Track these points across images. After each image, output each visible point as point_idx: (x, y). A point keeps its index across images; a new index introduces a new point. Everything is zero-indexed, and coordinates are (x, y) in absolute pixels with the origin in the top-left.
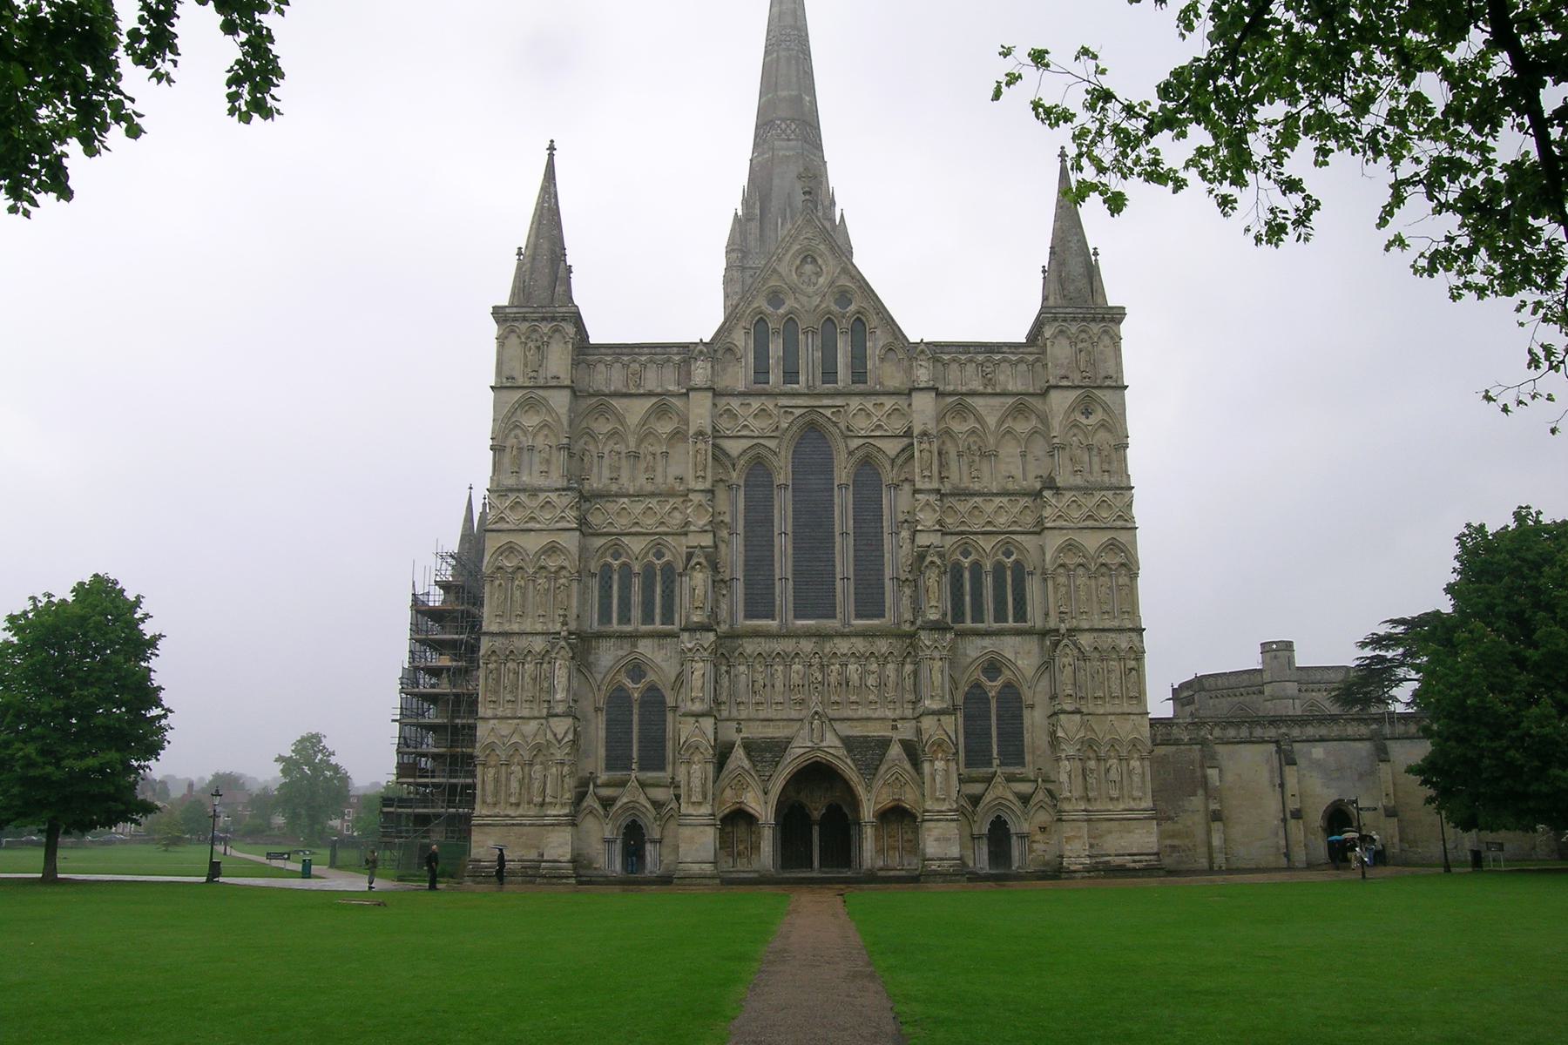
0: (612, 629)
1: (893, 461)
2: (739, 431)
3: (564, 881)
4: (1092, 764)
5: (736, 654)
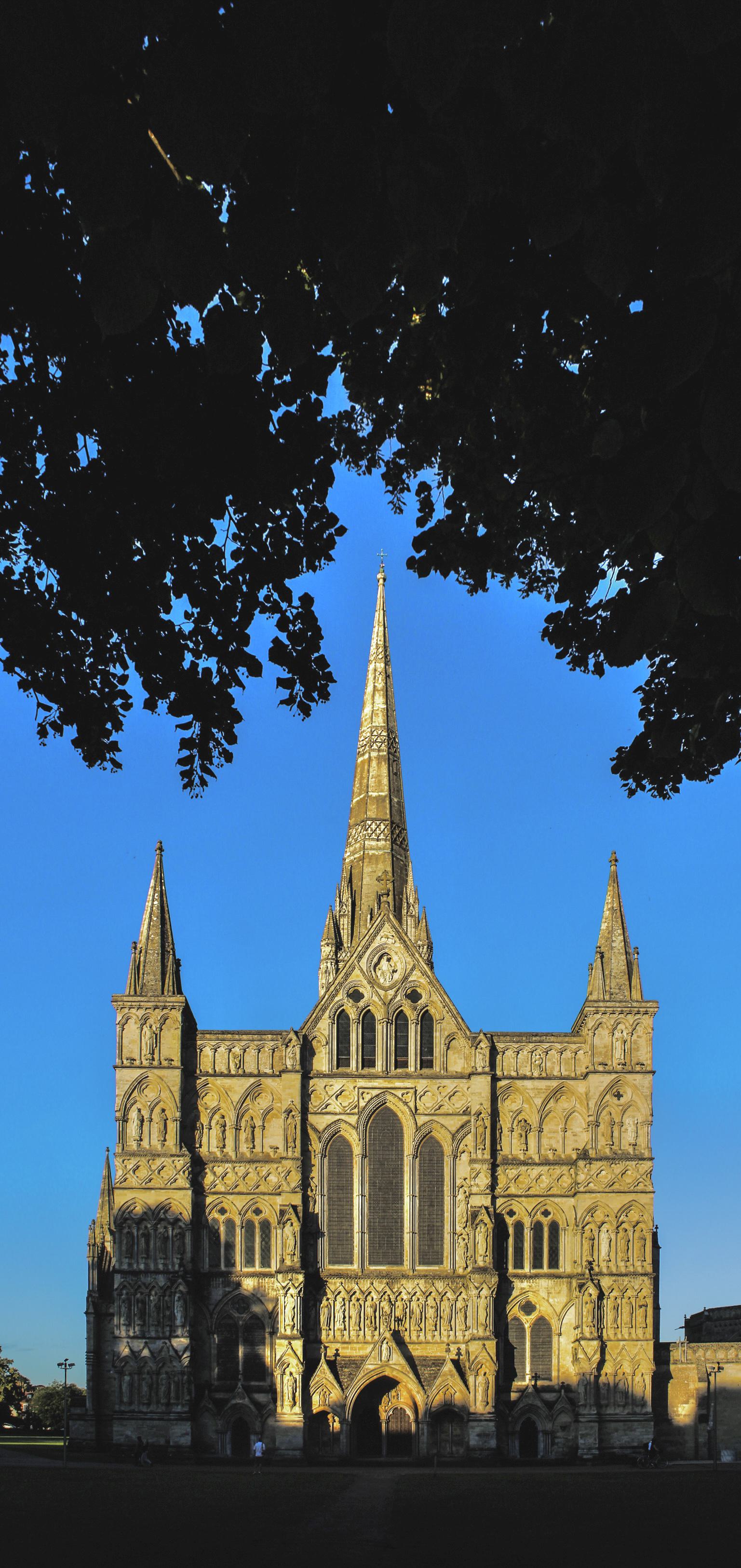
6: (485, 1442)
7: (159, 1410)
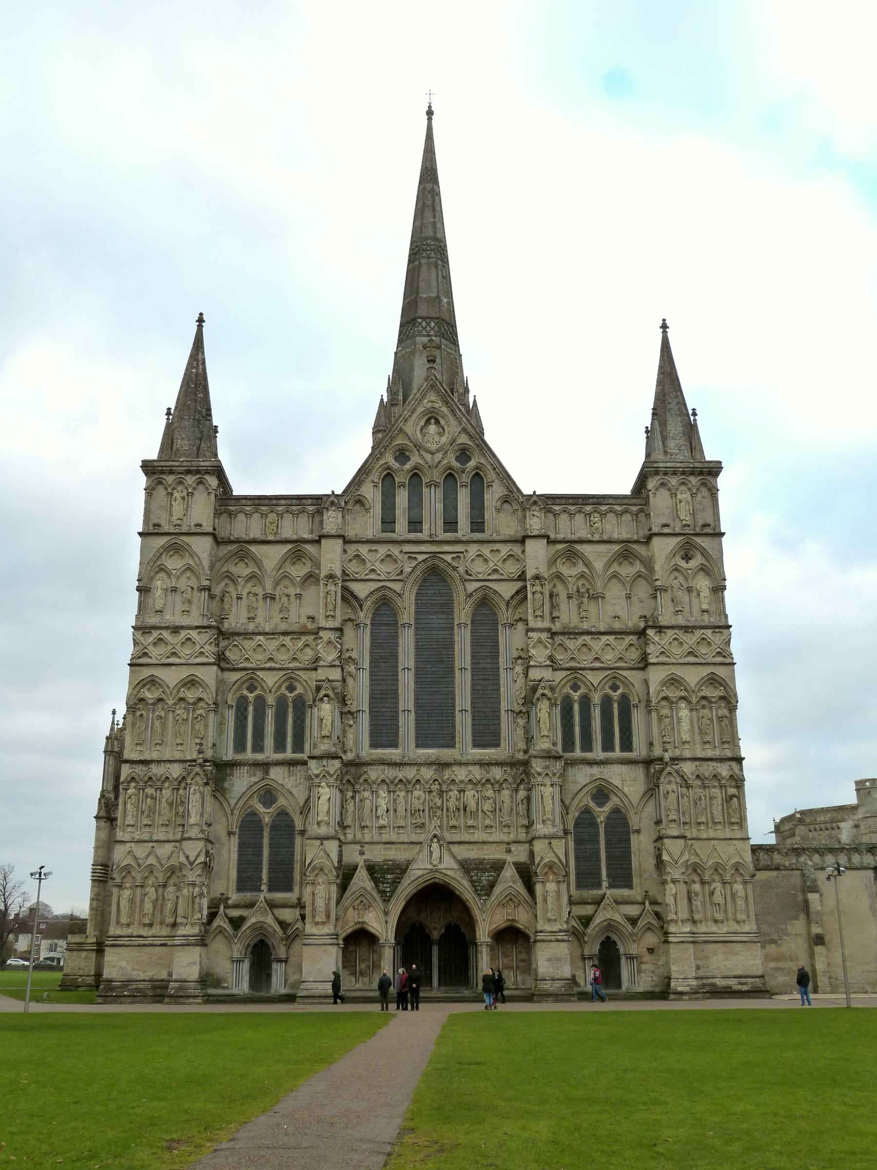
0: (246, 758)
1: (508, 604)
2: (366, 575)
3: (191, 1000)
4: (697, 887)
5: (361, 781)
6: (557, 969)
7: (163, 933)
